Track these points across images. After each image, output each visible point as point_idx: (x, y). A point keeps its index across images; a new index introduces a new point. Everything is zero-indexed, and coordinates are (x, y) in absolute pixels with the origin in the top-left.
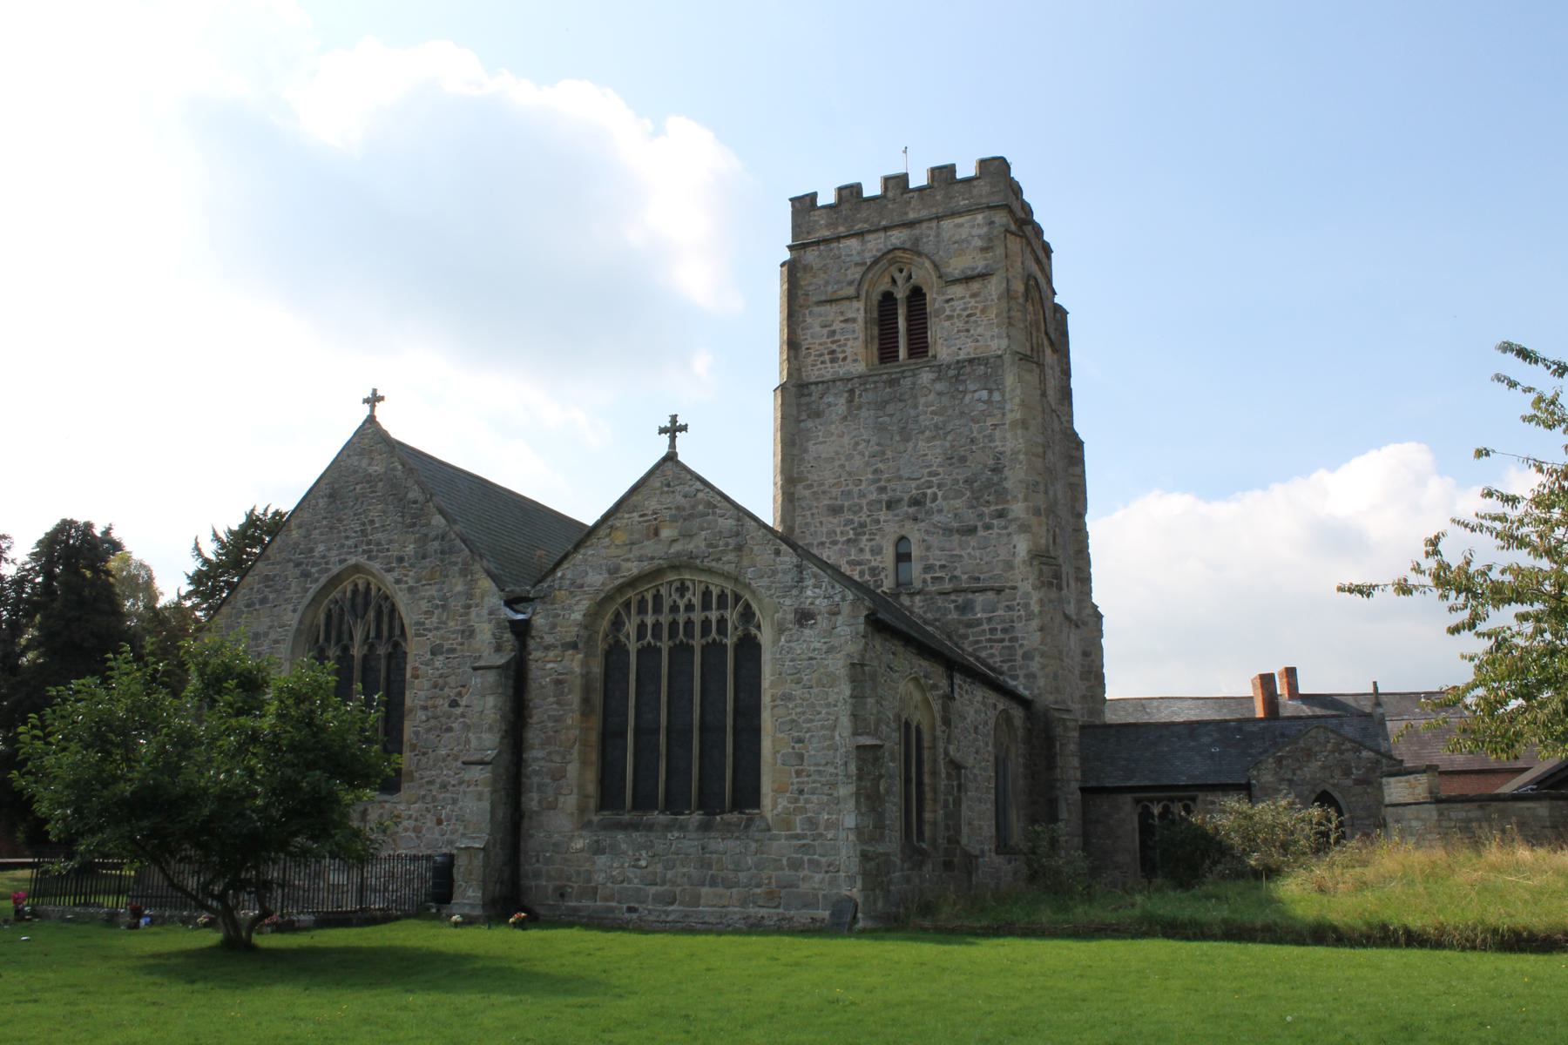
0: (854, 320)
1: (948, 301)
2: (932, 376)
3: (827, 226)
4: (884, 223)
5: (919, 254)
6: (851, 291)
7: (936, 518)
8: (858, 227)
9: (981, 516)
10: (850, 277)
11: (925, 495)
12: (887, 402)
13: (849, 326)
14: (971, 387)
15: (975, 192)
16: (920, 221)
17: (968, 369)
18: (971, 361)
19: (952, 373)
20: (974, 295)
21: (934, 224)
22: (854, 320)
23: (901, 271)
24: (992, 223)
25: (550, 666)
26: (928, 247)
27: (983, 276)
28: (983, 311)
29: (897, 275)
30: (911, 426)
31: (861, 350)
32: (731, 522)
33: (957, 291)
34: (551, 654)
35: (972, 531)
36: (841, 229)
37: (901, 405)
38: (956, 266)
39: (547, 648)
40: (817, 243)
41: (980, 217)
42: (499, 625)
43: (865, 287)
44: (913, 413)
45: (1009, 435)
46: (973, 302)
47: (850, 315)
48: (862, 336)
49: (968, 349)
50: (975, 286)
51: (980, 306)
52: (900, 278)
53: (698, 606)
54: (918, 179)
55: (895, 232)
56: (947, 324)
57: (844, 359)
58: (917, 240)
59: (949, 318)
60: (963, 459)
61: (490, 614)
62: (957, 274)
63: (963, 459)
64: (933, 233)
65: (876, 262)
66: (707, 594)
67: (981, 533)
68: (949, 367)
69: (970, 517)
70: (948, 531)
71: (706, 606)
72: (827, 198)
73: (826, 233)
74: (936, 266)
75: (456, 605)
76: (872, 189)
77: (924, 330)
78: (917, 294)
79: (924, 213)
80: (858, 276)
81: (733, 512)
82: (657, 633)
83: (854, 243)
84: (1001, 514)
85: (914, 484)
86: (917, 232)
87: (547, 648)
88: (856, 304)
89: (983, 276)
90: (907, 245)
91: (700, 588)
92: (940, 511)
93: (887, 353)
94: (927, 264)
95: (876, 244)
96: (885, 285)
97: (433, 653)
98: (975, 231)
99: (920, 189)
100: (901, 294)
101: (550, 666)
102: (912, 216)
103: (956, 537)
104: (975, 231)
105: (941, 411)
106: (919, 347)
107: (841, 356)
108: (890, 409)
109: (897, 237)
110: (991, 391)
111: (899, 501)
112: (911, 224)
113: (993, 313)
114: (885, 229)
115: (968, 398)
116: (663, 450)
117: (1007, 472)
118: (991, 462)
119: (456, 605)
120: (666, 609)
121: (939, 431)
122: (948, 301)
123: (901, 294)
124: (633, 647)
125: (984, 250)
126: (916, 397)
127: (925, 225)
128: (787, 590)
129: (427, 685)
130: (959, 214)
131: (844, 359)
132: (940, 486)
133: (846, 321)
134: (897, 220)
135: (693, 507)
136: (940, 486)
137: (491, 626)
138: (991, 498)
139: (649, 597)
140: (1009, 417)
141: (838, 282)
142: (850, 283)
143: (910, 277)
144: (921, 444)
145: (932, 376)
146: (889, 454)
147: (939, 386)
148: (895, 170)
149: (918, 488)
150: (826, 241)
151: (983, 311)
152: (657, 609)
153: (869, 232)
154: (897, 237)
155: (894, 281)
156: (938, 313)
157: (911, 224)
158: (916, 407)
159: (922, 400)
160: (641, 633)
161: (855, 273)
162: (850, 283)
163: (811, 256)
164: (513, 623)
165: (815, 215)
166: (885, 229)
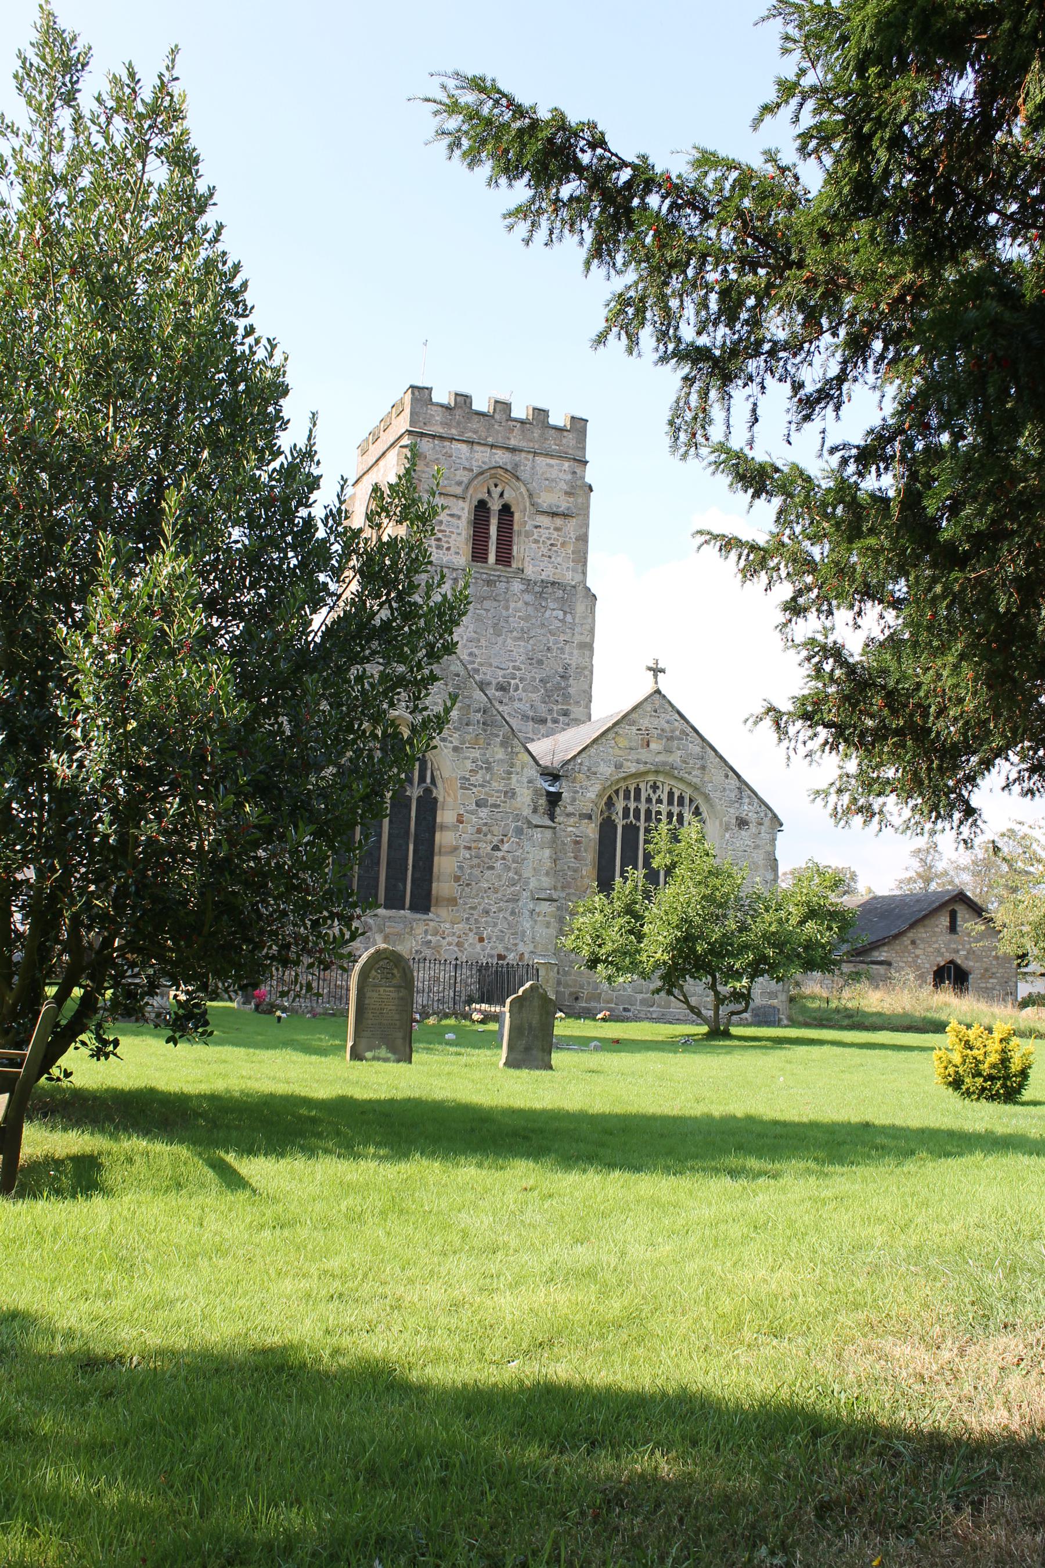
0: (459, 517)
1: (536, 527)
2: (523, 587)
3: (444, 424)
4: (490, 440)
5: (518, 479)
6: (458, 490)
7: (517, 705)
8: (469, 435)
9: (550, 711)
10: (458, 478)
11: (509, 684)
12: (485, 598)
13: (454, 521)
14: (551, 605)
15: (564, 441)
16: (521, 451)
17: (550, 590)
18: (553, 583)
19: (537, 589)
20: (557, 529)
21: (530, 457)
22: (459, 517)
23: (496, 486)
24: (575, 473)
25: (570, 829)
26: (524, 473)
27: (565, 515)
28: (563, 544)
29: (493, 488)
30: (502, 624)
31: (463, 546)
32: (698, 749)
33: (544, 521)
34: (572, 820)
35: (543, 721)
36: (454, 431)
37: (496, 604)
38: (546, 500)
39: (569, 815)
40: (434, 437)
41: (566, 464)
42: (537, 792)
43: (471, 491)
44: (504, 613)
45: (575, 652)
46: (555, 534)
47: (455, 511)
48: (464, 533)
49: (548, 574)
50: (559, 522)
51: (561, 540)
52: (496, 492)
53: (665, 801)
54: (519, 412)
55: (499, 452)
56: (534, 546)
57: (448, 549)
58: (516, 466)
59: (536, 541)
60: (540, 662)
61: (529, 782)
62: (545, 507)
63: (540, 662)
64: (529, 464)
65: (482, 473)
66: (671, 794)
67: (550, 724)
68: (535, 583)
69: (542, 710)
70: (525, 718)
71: (670, 802)
72: (441, 396)
73: (440, 430)
74: (531, 495)
75: (499, 770)
76: (481, 404)
77: (510, 545)
78: (506, 510)
79: (523, 444)
80: (465, 480)
81: (699, 741)
82: (637, 817)
83: (464, 447)
84: (566, 713)
85: (501, 673)
86: (517, 458)
87: (569, 815)
88: (460, 503)
89: (565, 515)
90: (509, 468)
91: (667, 789)
92: (520, 700)
93: (479, 554)
94: (523, 489)
95: (482, 457)
96: (483, 495)
97: (477, 805)
98: (562, 475)
99: (522, 422)
100: (495, 506)
101: (570, 829)
102: (513, 442)
103: (531, 723)
104: (562, 475)
105: (527, 618)
106: (505, 557)
107: (446, 545)
108: (487, 604)
109: (501, 457)
110: (565, 613)
111: (489, 684)
112: (513, 450)
113: (570, 549)
114: (492, 446)
115: (548, 614)
116: (648, 688)
117: (571, 681)
118: (560, 670)
119: (499, 770)
120: (643, 799)
121: (524, 635)
122: (536, 527)
123: (495, 506)
124: (620, 823)
125: (568, 494)
126: (507, 601)
127: (523, 455)
128: (732, 803)
129: (471, 830)
130: (552, 456)
131: (448, 549)
132: (521, 679)
133: (452, 515)
134: (500, 441)
135: (672, 731)
136: (521, 679)
137: (530, 792)
138: (560, 699)
139: (632, 789)
140: (577, 638)
141: (448, 479)
142: (459, 483)
143: (502, 495)
144: (509, 641)
145: (523, 587)
146: (483, 643)
147: (528, 597)
148: (502, 397)
149: (504, 677)
150: (442, 438)
151: (563, 544)
152: (637, 798)
153: (479, 443)
154: (501, 457)
155: (489, 492)
156: (528, 534)
157: (513, 450)
158: (507, 608)
159: (512, 605)
160: (626, 815)
161: (464, 476)
162: (459, 483)
163: (426, 446)
164: (549, 794)
165: (433, 410)
166: (492, 446)
